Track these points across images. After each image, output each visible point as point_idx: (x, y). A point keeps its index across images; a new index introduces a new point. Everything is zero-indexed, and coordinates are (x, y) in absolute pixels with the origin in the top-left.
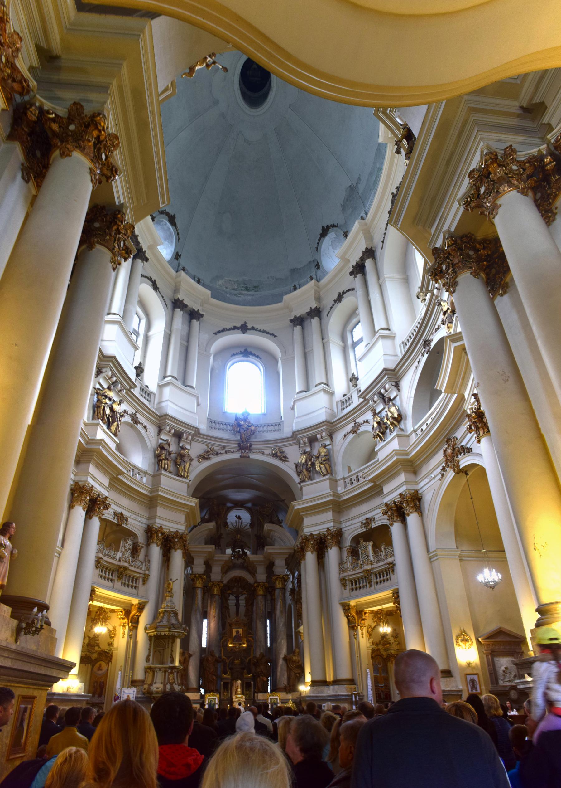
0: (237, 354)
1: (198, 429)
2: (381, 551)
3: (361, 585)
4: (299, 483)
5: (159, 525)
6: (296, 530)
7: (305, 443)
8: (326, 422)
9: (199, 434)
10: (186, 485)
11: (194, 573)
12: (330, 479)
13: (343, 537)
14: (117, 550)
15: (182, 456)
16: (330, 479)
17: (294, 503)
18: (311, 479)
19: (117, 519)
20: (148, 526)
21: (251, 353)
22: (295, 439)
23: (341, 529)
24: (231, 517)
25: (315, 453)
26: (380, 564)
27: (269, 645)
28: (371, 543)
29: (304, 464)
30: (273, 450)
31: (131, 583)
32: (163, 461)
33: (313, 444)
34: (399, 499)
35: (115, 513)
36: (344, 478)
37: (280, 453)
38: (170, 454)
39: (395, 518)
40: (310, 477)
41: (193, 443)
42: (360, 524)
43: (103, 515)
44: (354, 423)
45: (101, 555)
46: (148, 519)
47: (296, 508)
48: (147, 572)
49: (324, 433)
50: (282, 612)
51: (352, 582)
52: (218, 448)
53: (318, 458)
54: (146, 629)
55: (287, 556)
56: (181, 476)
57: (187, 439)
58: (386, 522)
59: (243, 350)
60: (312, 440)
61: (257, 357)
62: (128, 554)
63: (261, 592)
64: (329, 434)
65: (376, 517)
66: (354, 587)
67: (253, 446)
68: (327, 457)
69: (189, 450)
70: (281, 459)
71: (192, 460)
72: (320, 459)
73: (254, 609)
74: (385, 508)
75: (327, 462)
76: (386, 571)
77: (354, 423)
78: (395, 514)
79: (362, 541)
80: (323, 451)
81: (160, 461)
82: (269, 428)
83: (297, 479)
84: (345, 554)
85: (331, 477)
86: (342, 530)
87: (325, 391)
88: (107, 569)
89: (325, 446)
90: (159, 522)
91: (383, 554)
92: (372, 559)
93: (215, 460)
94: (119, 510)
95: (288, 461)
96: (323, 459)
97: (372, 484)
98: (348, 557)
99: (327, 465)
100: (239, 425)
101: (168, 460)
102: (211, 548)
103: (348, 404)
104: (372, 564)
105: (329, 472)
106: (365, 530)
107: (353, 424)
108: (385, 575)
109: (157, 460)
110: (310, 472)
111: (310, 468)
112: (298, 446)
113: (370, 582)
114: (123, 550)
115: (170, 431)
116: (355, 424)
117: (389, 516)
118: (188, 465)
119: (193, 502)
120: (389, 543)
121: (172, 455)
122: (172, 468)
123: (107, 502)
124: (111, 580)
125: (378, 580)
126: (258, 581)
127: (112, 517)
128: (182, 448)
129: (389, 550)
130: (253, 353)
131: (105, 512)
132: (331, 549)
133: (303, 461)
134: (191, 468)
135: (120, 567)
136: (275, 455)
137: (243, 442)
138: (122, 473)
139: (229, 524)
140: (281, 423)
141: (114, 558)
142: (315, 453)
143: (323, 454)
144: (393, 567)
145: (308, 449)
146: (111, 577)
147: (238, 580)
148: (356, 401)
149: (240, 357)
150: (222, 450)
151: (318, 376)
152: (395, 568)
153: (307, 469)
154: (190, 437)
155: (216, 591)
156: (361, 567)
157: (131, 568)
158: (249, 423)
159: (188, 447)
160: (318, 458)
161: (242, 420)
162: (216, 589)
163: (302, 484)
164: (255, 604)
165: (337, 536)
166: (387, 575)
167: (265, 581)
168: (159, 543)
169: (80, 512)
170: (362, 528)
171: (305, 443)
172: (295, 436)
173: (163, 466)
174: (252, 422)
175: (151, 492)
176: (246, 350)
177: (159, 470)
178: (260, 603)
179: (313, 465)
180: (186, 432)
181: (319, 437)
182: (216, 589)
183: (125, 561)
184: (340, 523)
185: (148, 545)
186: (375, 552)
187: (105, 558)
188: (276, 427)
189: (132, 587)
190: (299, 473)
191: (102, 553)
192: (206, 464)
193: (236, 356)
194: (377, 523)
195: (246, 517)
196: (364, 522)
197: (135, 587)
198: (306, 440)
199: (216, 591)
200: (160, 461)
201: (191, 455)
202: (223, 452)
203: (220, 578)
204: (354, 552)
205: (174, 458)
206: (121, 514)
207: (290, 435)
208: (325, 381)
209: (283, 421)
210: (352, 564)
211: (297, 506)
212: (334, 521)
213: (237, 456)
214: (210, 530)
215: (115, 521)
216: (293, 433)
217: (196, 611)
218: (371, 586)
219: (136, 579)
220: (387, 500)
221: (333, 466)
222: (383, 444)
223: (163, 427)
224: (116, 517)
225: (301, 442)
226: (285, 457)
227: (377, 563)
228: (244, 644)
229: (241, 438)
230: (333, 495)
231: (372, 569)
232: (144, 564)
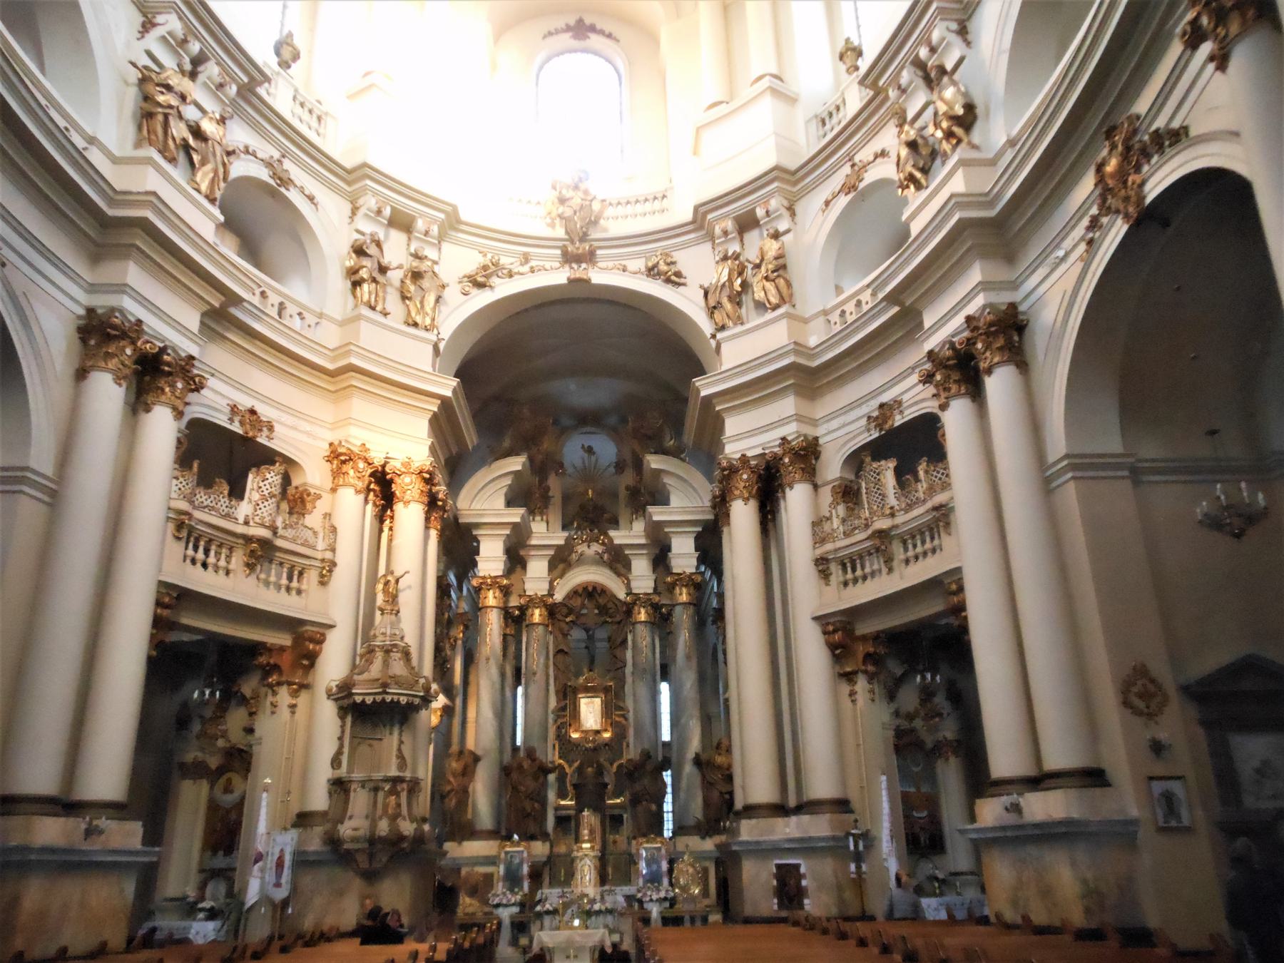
0: (557, 32)
1: (455, 208)
2: (917, 480)
3: (868, 570)
4: (714, 336)
5: (359, 443)
6: (705, 448)
7: (726, 233)
8: (778, 173)
9: (459, 222)
10: (430, 348)
11: (481, 574)
12: (787, 315)
13: (823, 457)
14: (237, 492)
15: (416, 276)
16: (787, 315)
17: (698, 382)
18: (739, 321)
19: (242, 423)
20: (331, 444)
21: (593, 29)
22: (701, 228)
23: (816, 439)
24: (572, 451)
25: (751, 254)
26: (916, 512)
27: (666, 736)
28: (892, 464)
29: (724, 285)
30: (647, 259)
31: (284, 581)
32: (365, 286)
33: (747, 236)
34: (966, 334)
35: (234, 409)
36: (825, 313)
37: (668, 264)
38: (383, 270)
39: (954, 388)
40: (739, 318)
41: (445, 246)
42: (864, 422)
43: (187, 404)
44: (849, 164)
45: (183, 505)
46: (332, 430)
47: (703, 393)
48: (328, 555)
49: (774, 203)
50: (688, 657)
51: (844, 566)
52: (512, 260)
53: (758, 266)
54: (329, 695)
55: (700, 529)
56: (415, 325)
57: (426, 233)
58: (931, 406)
59: (572, 22)
60: (746, 223)
61: (609, 36)
62: (269, 507)
63: (643, 616)
64: (786, 203)
65: (905, 397)
66: (850, 576)
67: (599, 252)
68: (781, 261)
69: (435, 263)
70: (668, 281)
71: (443, 287)
72: (763, 269)
73: (629, 654)
74: (928, 366)
75: (781, 272)
76: (931, 530)
77: (849, 164)
78: (956, 376)
79: (868, 459)
80: (772, 247)
81: (356, 284)
82: (639, 208)
83: (706, 327)
84: (826, 495)
85: (791, 310)
86: (821, 441)
87: (774, 91)
88: (210, 541)
89: (776, 236)
90: (355, 437)
91: (922, 487)
92: (892, 501)
93: (503, 289)
94: (245, 402)
95: (684, 284)
96: (771, 267)
97: (896, 309)
98: (834, 504)
99: (781, 282)
100: (562, 201)
101: (374, 280)
102: (516, 515)
103: (835, 120)
104: (892, 515)
105: (787, 299)
106: (877, 435)
107: (847, 169)
108: (928, 539)
109: (349, 284)
110: (739, 304)
111: (739, 294)
112: (708, 246)
113: (889, 561)
114: (256, 496)
115: (379, 212)
116: (853, 166)
117: (936, 386)
118: (431, 299)
119: (447, 386)
120: (937, 453)
121: (389, 273)
122: (392, 301)
123: (196, 372)
124: (228, 573)
125: (911, 553)
126: (635, 591)
127: (226, 418)
128: (416, 256)
129: (937, 476)
130: (598, 27)
131: (192, 397)
132: (792, 488)
133: (724, 278)
134: (444, 309)
135: (248, 539)
136: (652, 272)
137: (572, 242)
138: (237, 300)
139: (566, 464)
140: (668, 194)
141: (227, 516)
142: (751, 254)
143: (771, 254)
144: (946, 516)
145: (734, 247)
146: (222, 563)
147: (591, 592)
148: (855, 99)
149: (566, 39)
150: (522, 265)
151: (759, 58)
152: (952, 517)
153: (730, 298)
154: (435, 230)
155: (537, 615)
156: (867, 526)
157: (279, 543)
158: (586, 192)
159: (430, 253)
160: (758, 266)
161: (568, 187)
162: (537, 612)
163: (719, 336)
164: (630, 642)
165: (806, 455)
166: (932, 538)
167: (651, 591)
168: (360, 485)
169: (106, 392)
170: (869, 430)
171: (726, 233)
172: (700, 222)
173: (366, 298)
174: (593, 192)
175: (333, 360)
176: (580, 21)
177: (356, 306)
178: (642, 638)
179: (745, 285)
180: (422, 215)
181: (760, 212)
182: (537, 612)
183: (263, 525)
184: (814, 423)
185: (334, 490)
186: (901, 483)
187: (198, 514)
188: (657, 205)
189: (288, 589)
190: (712, 311)
191: (191, 502)
192: (482, 299)
193: (555, 38)
194: (906, 413)
195: (607, 449)
196: (875, 414)
197: (299, 592)
198: (729, 225)
199: (537, 615)
200: (356, 284)
201: (441, 275)
202: (526, 268)
203: (546, 586)
204: (848, 493)
205: (397, 284)
206: (253, 412)
207: (688, 216)
208: (774, 71)
209: (672, 188)
210: (844, 521)
211: (706, 387)
212: (799, 418)
213: (558, 277)
214: (516, 473)
215: (236, 428)
216: (696, 209)
217: (488, 659)
218: (890, 570)
219: (301, 574)
220: (932, 343)
221: (795, 285)
222: (924, 194)
223: (361, 202)
224: (237, 419)
225: (718, 231)
226: (678, 274)
227: (906, 511)
228: (606, 730)
229: (567, 233)
230: (796, 352)
231: (895, 527)
232: (321, 536)
